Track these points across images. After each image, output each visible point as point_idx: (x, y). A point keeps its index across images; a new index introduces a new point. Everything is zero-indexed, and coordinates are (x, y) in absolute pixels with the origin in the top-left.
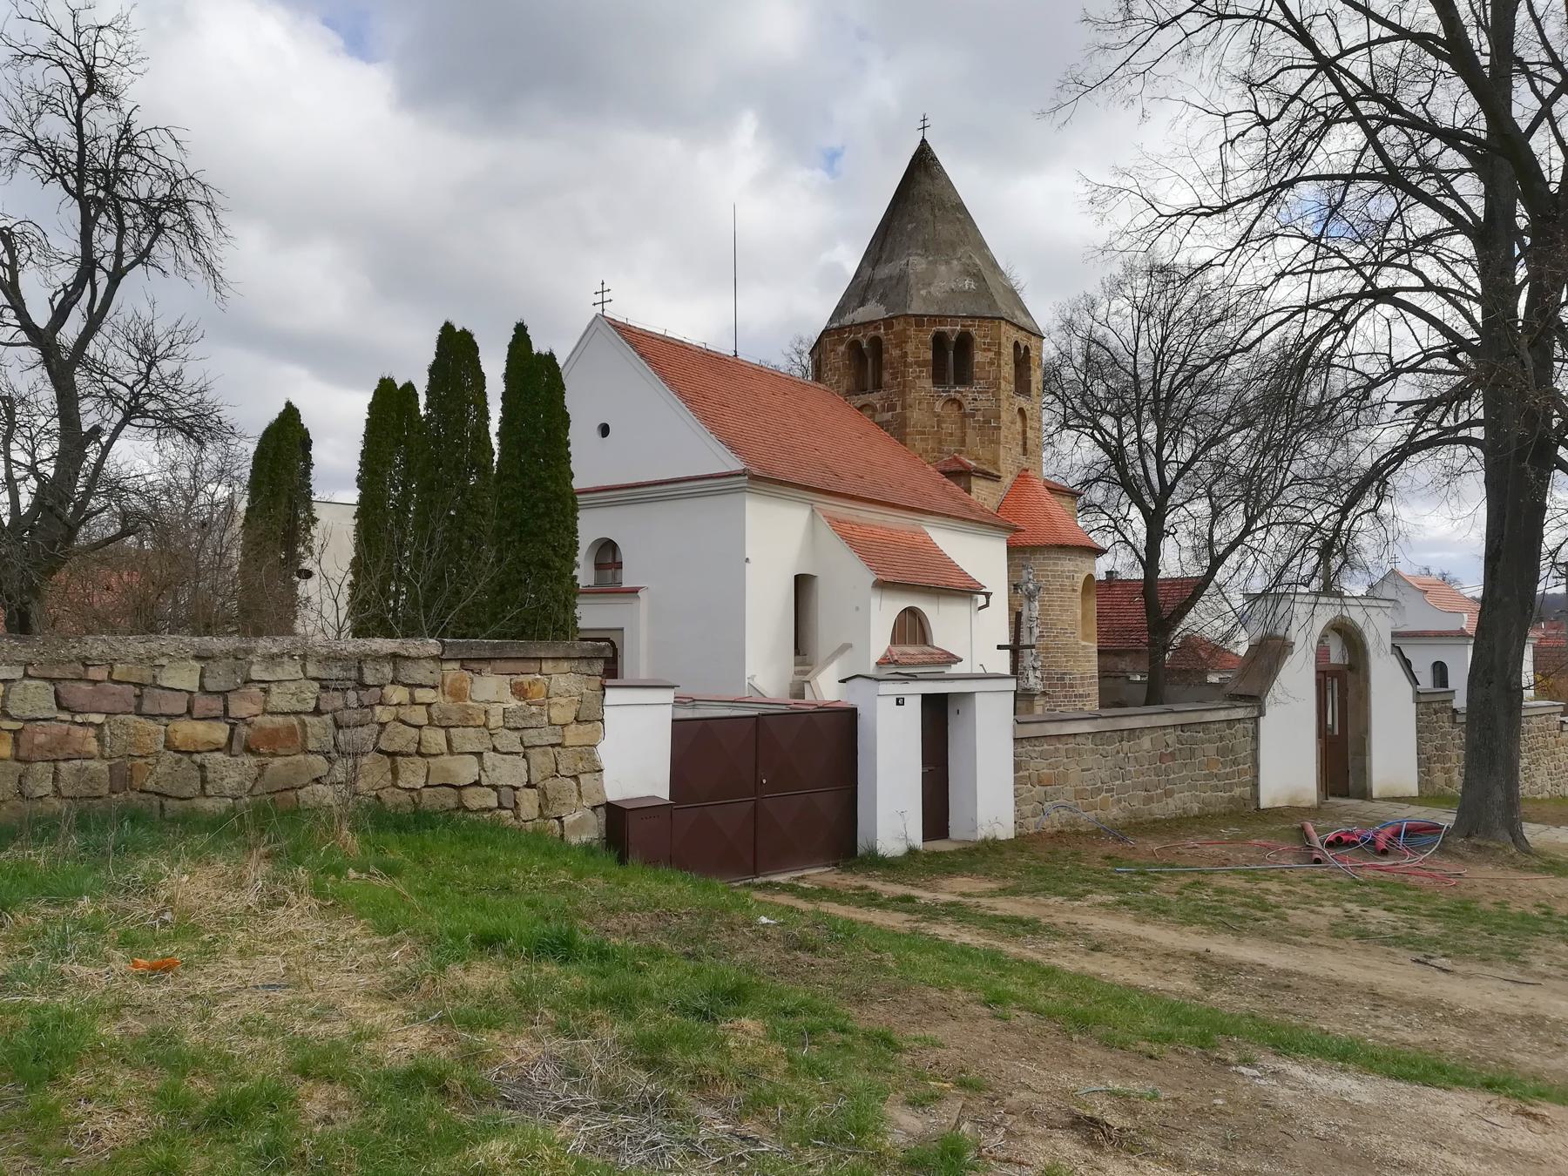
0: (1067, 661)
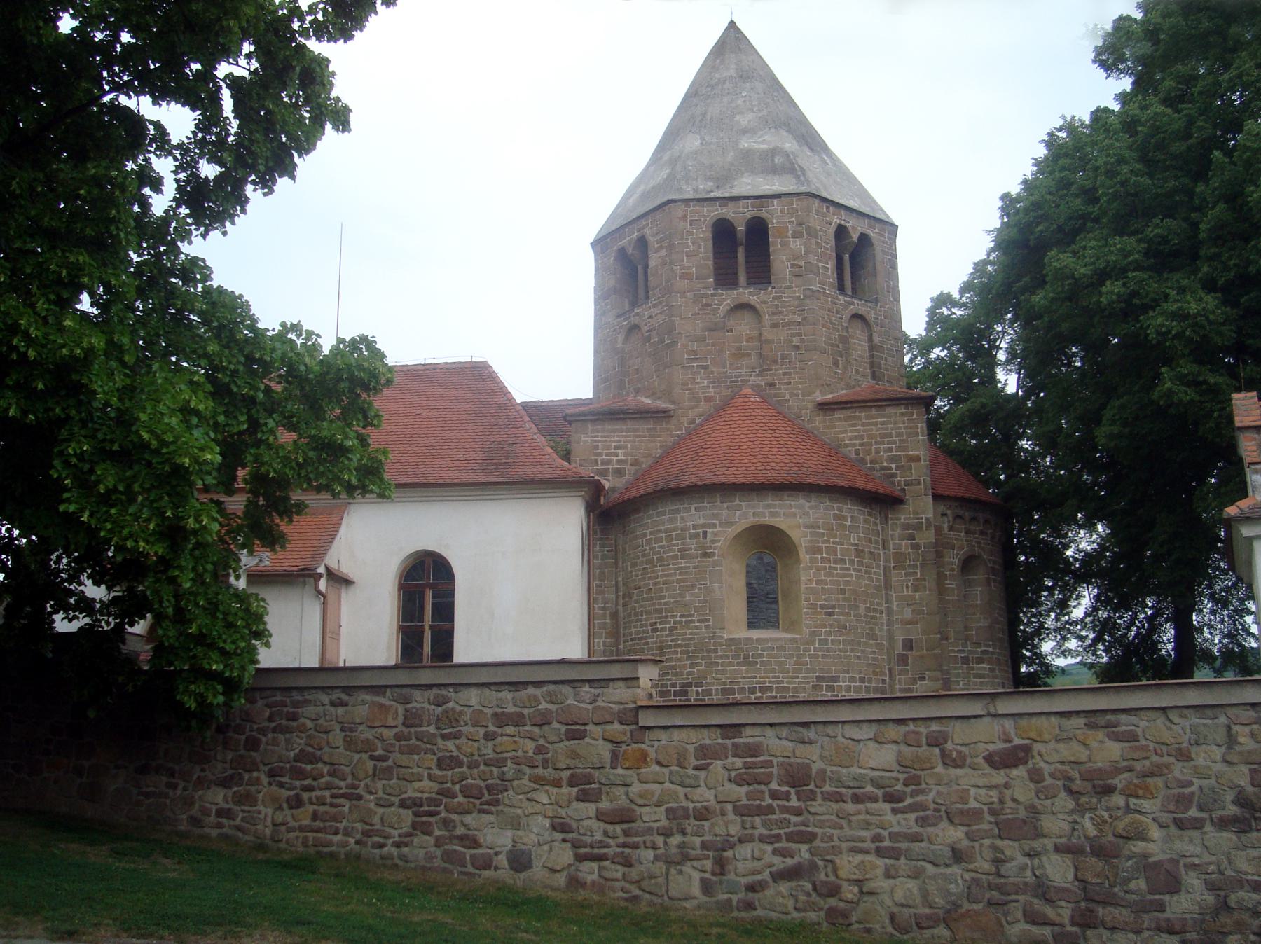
0: (692, 666)
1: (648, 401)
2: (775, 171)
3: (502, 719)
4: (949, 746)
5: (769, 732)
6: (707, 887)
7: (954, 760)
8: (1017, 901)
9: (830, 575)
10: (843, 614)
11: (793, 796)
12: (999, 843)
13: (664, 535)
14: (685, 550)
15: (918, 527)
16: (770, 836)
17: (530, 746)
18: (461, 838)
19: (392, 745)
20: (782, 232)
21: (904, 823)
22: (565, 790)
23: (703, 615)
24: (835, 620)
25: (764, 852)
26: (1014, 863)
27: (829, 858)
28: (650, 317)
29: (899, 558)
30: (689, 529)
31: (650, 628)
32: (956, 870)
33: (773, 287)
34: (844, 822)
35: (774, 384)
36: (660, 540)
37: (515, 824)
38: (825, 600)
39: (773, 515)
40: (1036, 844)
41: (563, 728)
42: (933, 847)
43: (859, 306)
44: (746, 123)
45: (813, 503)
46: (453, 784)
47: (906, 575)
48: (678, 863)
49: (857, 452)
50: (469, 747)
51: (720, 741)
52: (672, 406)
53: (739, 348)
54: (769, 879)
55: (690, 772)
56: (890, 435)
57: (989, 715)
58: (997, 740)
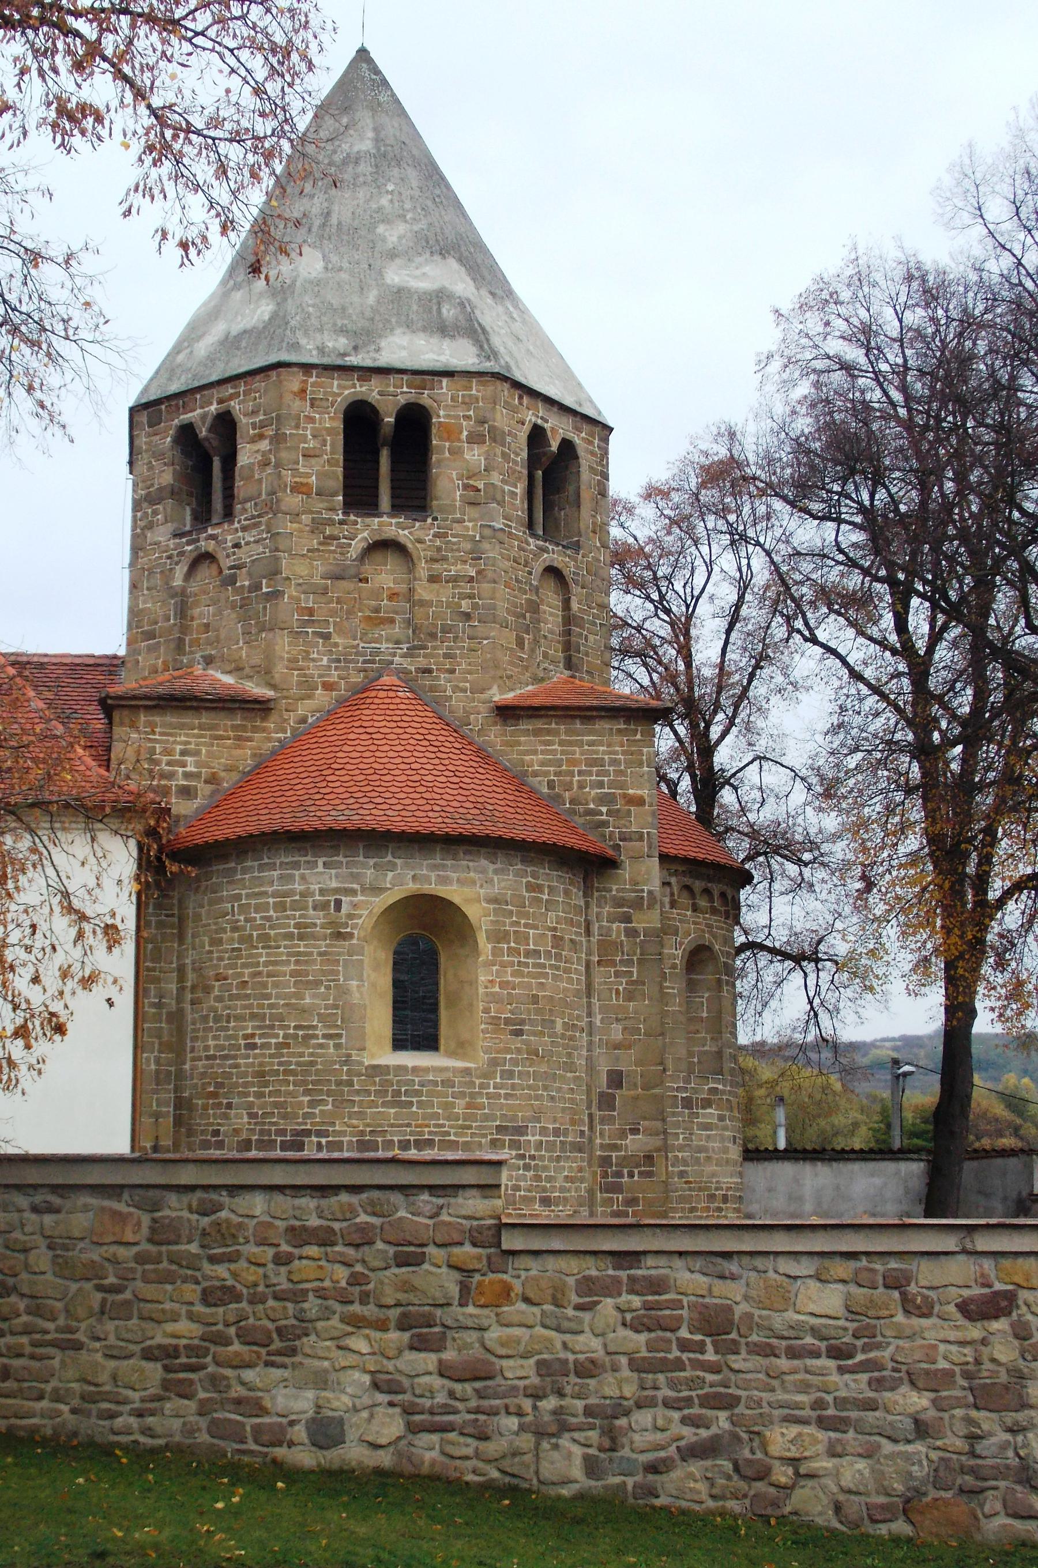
0: (312, 1104)
1: (228, 679)
2: (443, 330)
3: (300, 1235)
4: (913, 1288)
5: (678, 1263)
6: (592, 1467)
7: (919, 1307)
8: (996, 1488)
9: (521, 974)
10: (534, 1034)
11: (710, 1347)
12: (974, 1413)
13: (271, 900)
14: (306, 926)
15: (637, 904)
16: (679, 1399)
17: (342, 1274)
18: (239, 1402)
19: (133, 1270)
20: (451, 433)
21: (852, 1385)
22: (394, 1336)
23: (329, 1027)
24: (523, 1042)
25: (670, 1421)
26: (993, 1440)
27: (756, 1429)
28: (237, 546)
29: (607, 948)
30: (313, 894)
31: (242, 1042)
32: (919, 1447)
33: (435, 519)
34: (775, 1383)
35: (429, 671)
36: (265, 907)
37: (321, 1381)
38: (512, 1012)
39: (444, 881)
40: (1021, 1416)
41: (391, 1250)
42: (890, 1418)
43: (555, 556)
44: (395, 239)
45: (499, 865)
46: (227, 1325)
47: (617, 974)
48: (553, 1435)
49: (551, 785)
50: (252, 1274)
51: (611, 1272)
52: (270, 693)
53: (377, 610)
54: (676, 1457)
55: (570, 1312)
56: (600, 762)
57: (965, 1251)
58: (973, 1284)
